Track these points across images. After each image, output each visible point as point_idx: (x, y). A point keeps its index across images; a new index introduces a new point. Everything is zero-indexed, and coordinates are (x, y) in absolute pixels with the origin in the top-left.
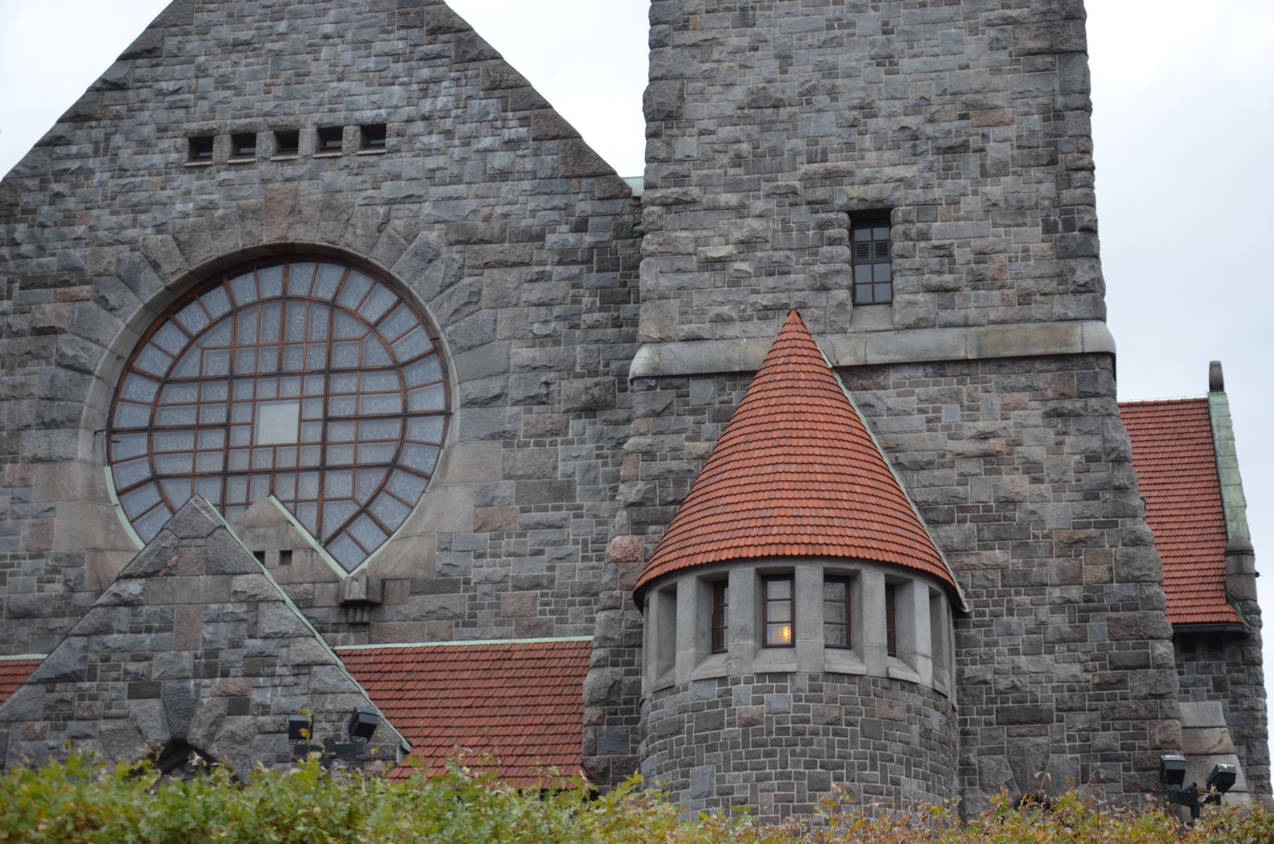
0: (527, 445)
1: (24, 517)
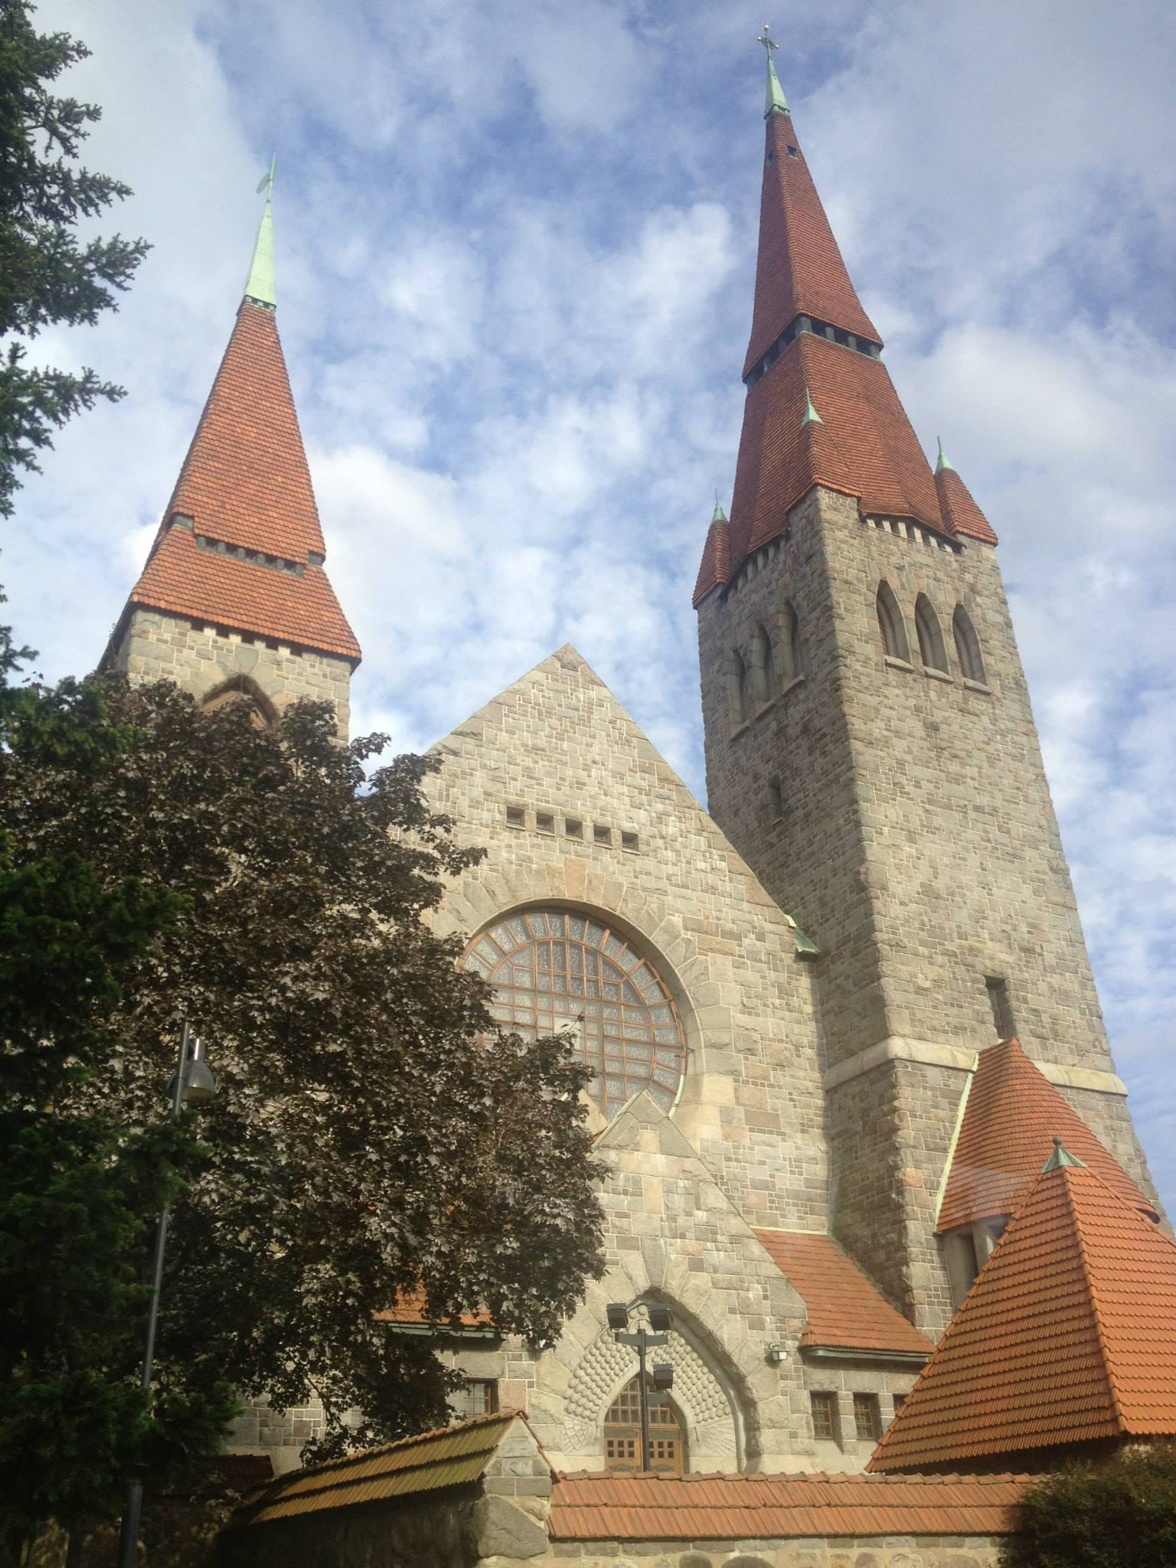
0: (748, 1082)
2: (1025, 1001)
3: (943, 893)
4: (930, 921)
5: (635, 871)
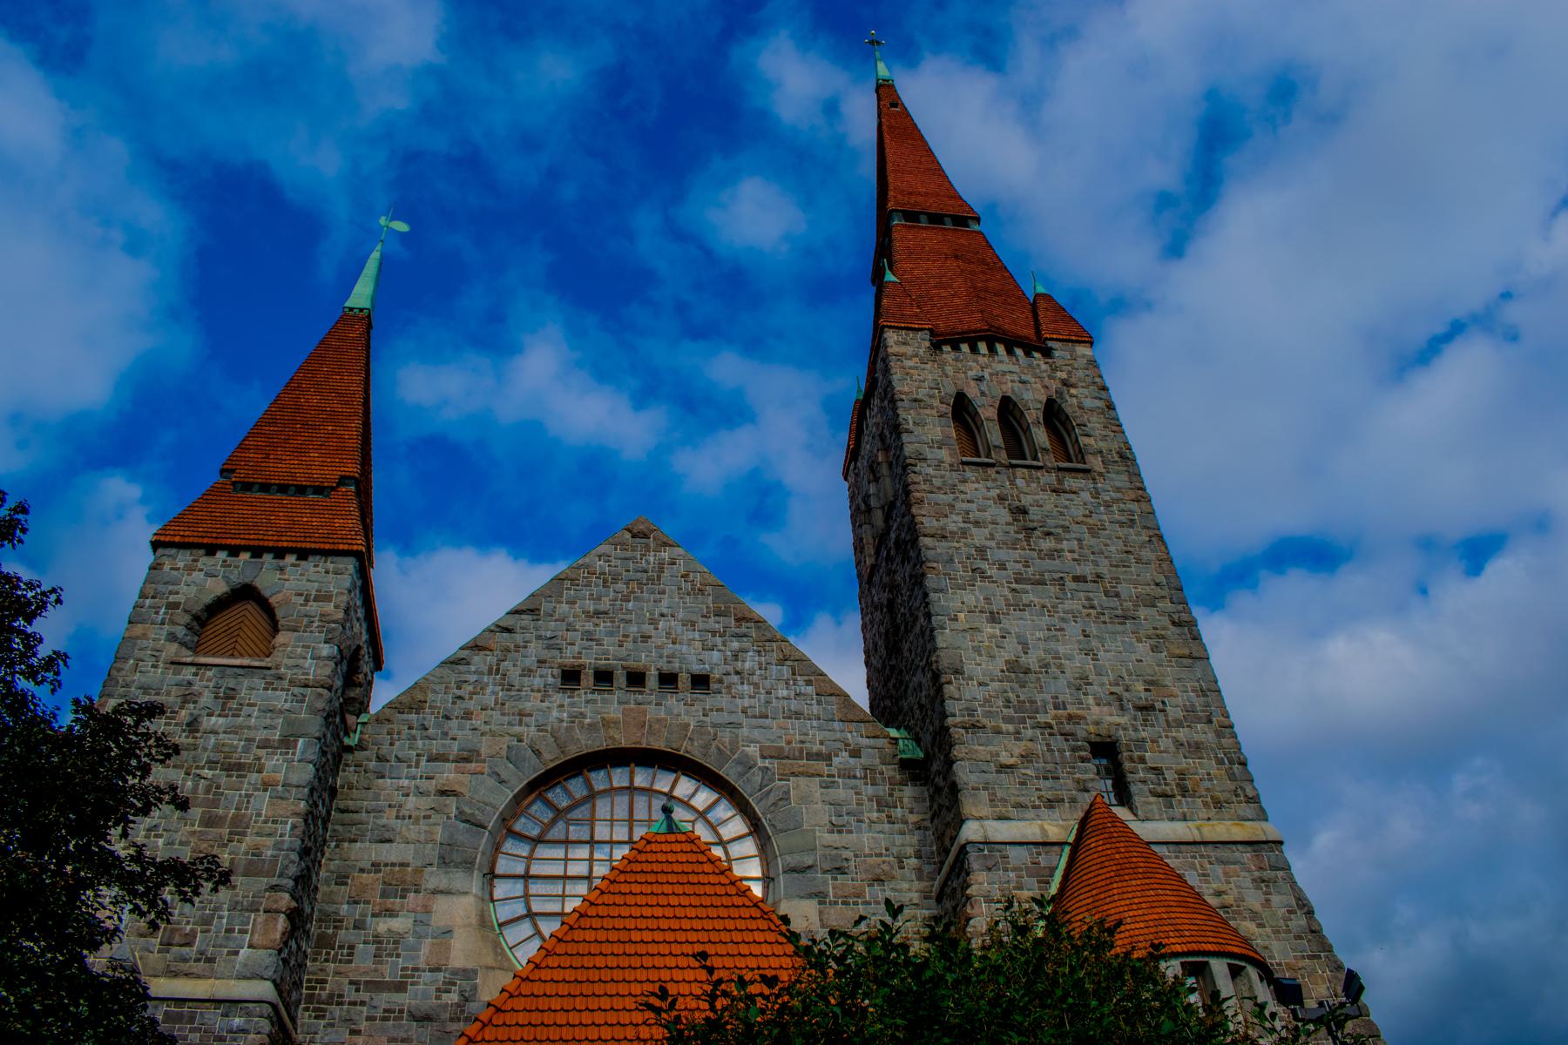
0: (836, 903)
1: (426, 936)
2: (1142, 760)
3: (1035, 666)
4: (1018, 696)
5: (704, 709)
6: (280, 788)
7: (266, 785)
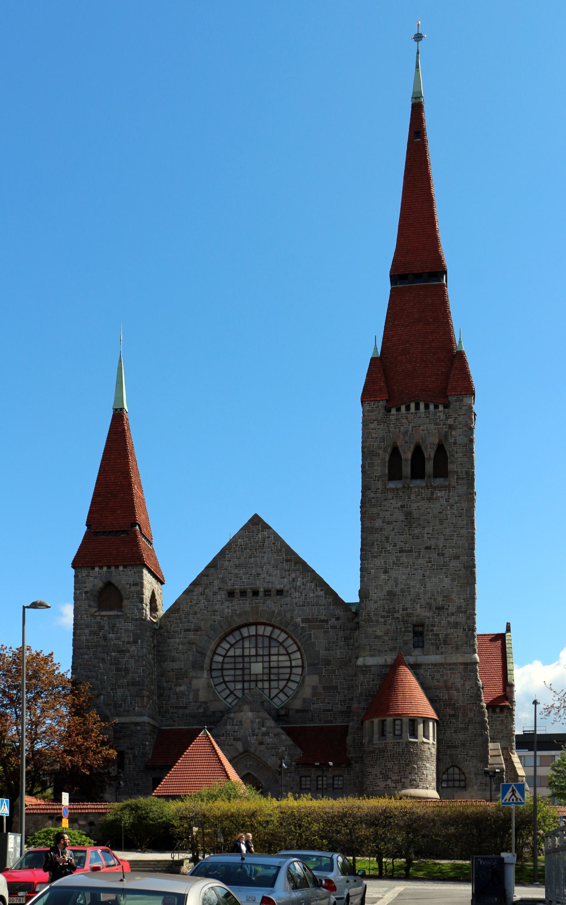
2: (432, 631)
5: (281, 605)
6: (136, 658)
7: (132, 657)
